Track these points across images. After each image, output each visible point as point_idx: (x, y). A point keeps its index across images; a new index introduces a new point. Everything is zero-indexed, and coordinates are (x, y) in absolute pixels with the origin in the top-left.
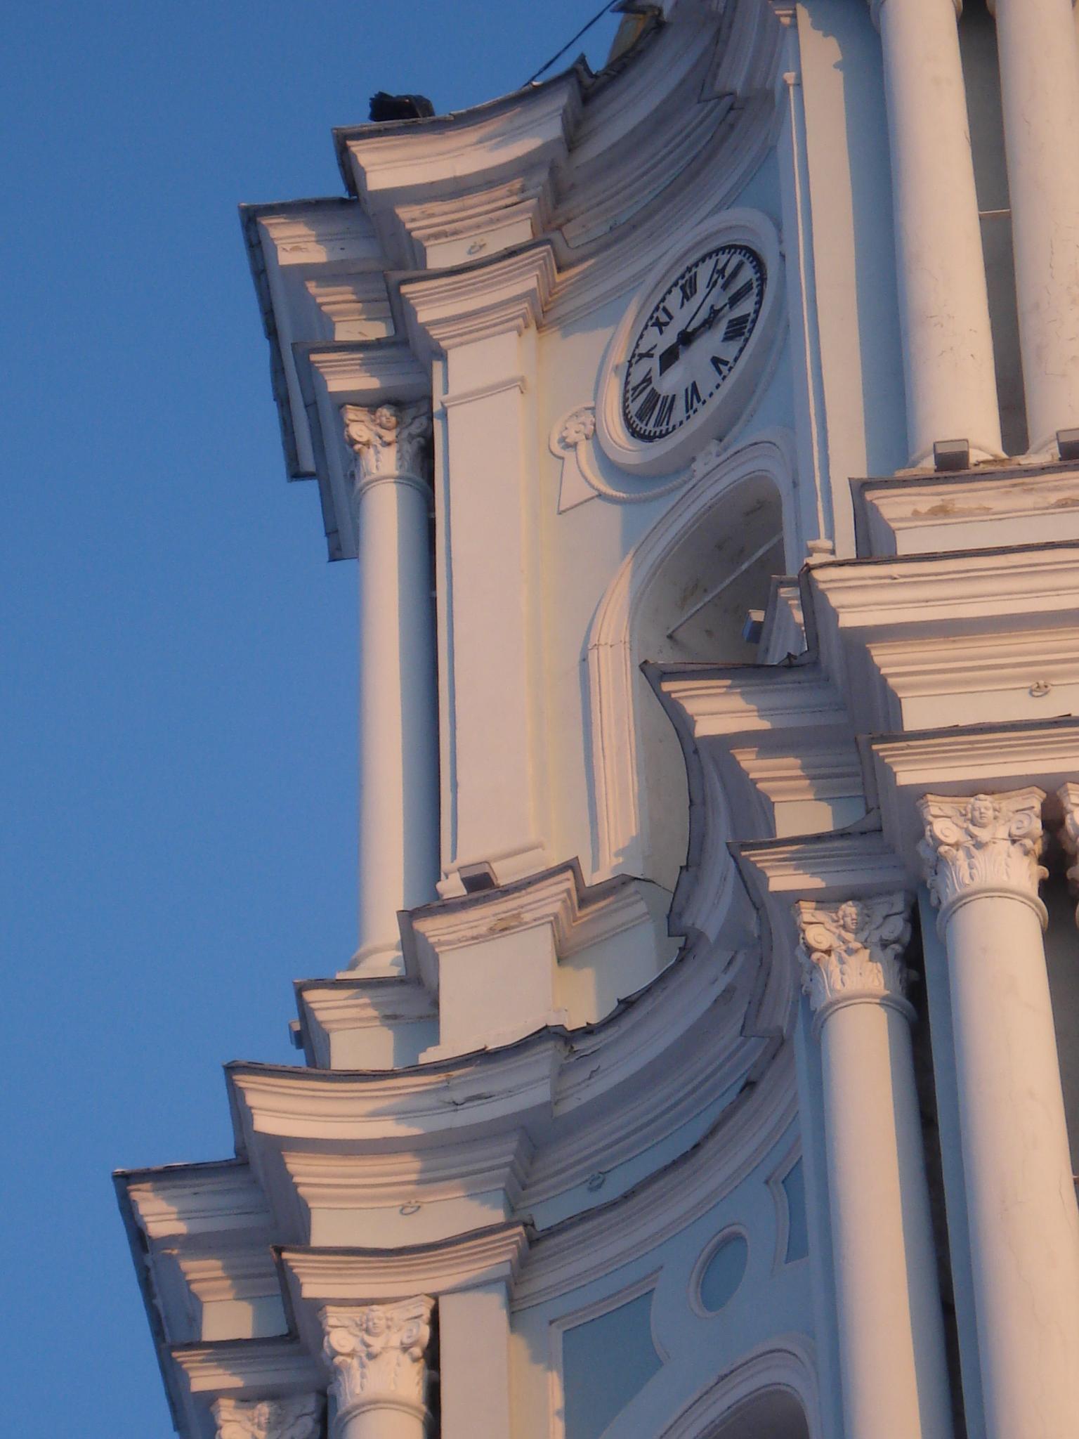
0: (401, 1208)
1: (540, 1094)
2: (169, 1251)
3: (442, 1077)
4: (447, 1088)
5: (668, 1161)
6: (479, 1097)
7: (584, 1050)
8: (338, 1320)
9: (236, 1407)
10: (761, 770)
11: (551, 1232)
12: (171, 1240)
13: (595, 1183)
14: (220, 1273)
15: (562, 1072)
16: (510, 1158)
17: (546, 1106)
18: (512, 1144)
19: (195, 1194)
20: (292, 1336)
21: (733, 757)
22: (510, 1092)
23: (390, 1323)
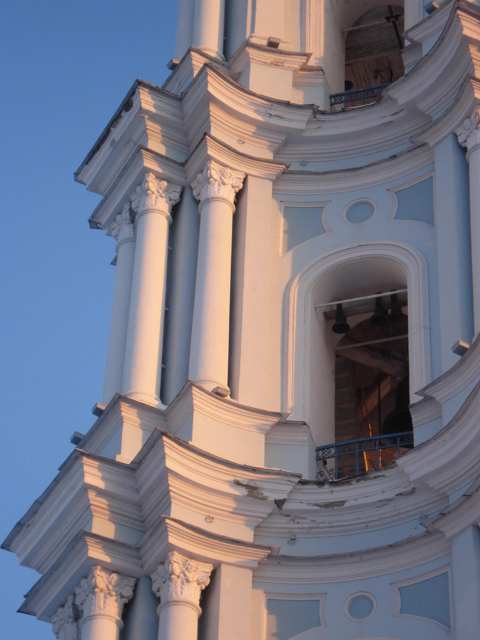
0: (238, 140)
1: (302, 126)
2: (143, 115)
3: (270, 104)
4: (270, 109)
5: (350, 167)
6: (279, 117)
7: (320, 118)
8: (214, 166)
9: (155, 179)
10: (476, 55)
11: (291, 173)
12: (147, 112)
13: (303, 163)
14: (159, 132)
15: (308, 122)
16: (280, 142)
17: (302, 131)
18: (283, 138)
19: (160, 100)
20: (183, 165)
21: (468, 46)
22: (291, 120)
23: (231, 176)
